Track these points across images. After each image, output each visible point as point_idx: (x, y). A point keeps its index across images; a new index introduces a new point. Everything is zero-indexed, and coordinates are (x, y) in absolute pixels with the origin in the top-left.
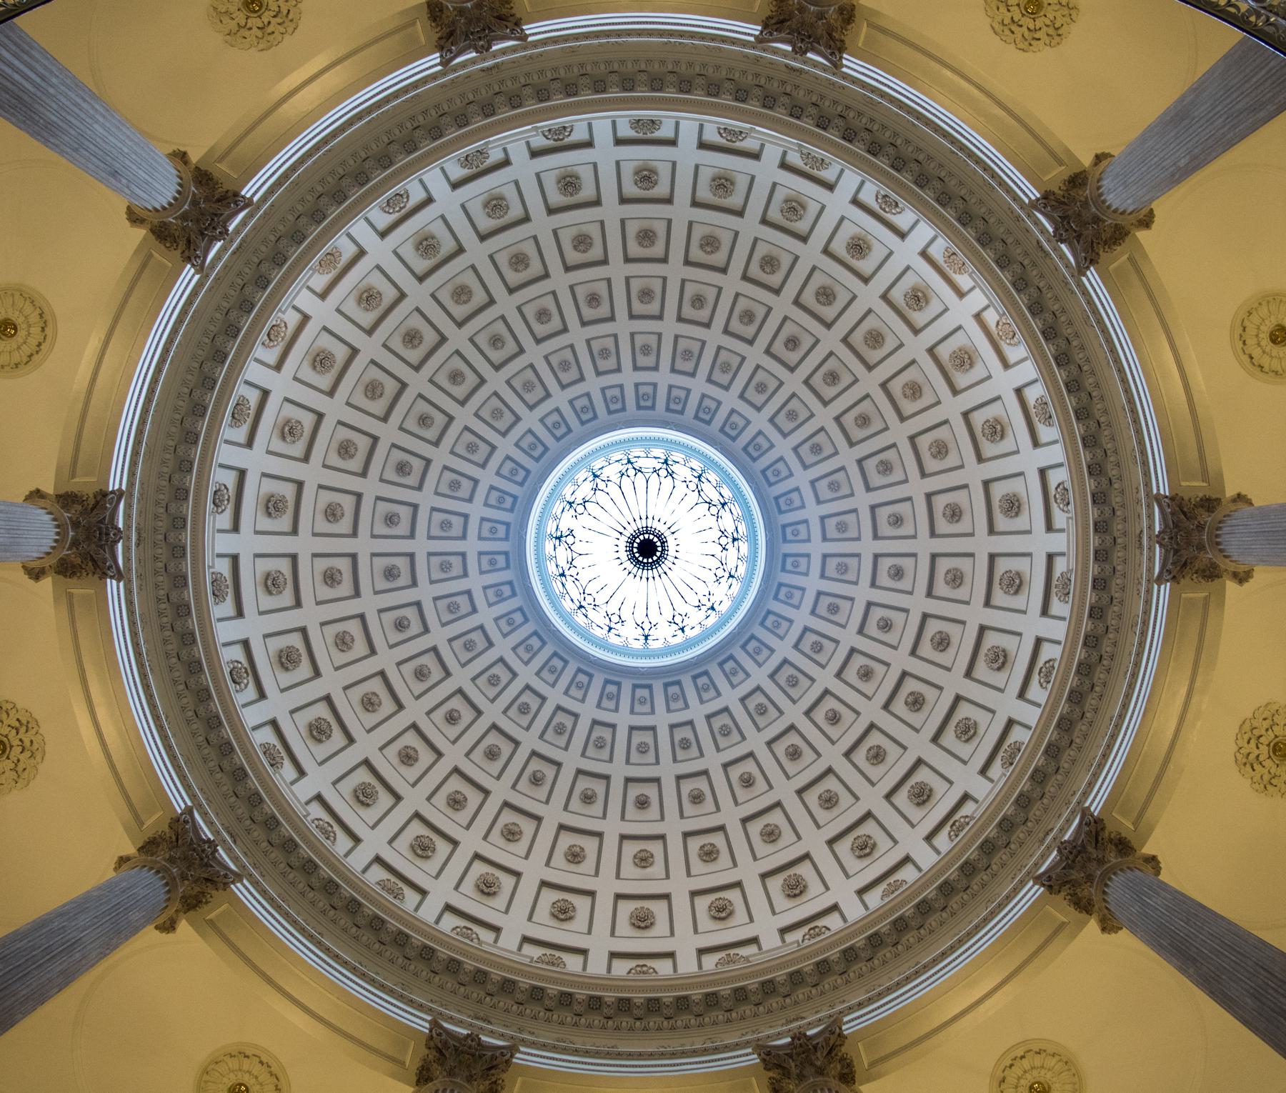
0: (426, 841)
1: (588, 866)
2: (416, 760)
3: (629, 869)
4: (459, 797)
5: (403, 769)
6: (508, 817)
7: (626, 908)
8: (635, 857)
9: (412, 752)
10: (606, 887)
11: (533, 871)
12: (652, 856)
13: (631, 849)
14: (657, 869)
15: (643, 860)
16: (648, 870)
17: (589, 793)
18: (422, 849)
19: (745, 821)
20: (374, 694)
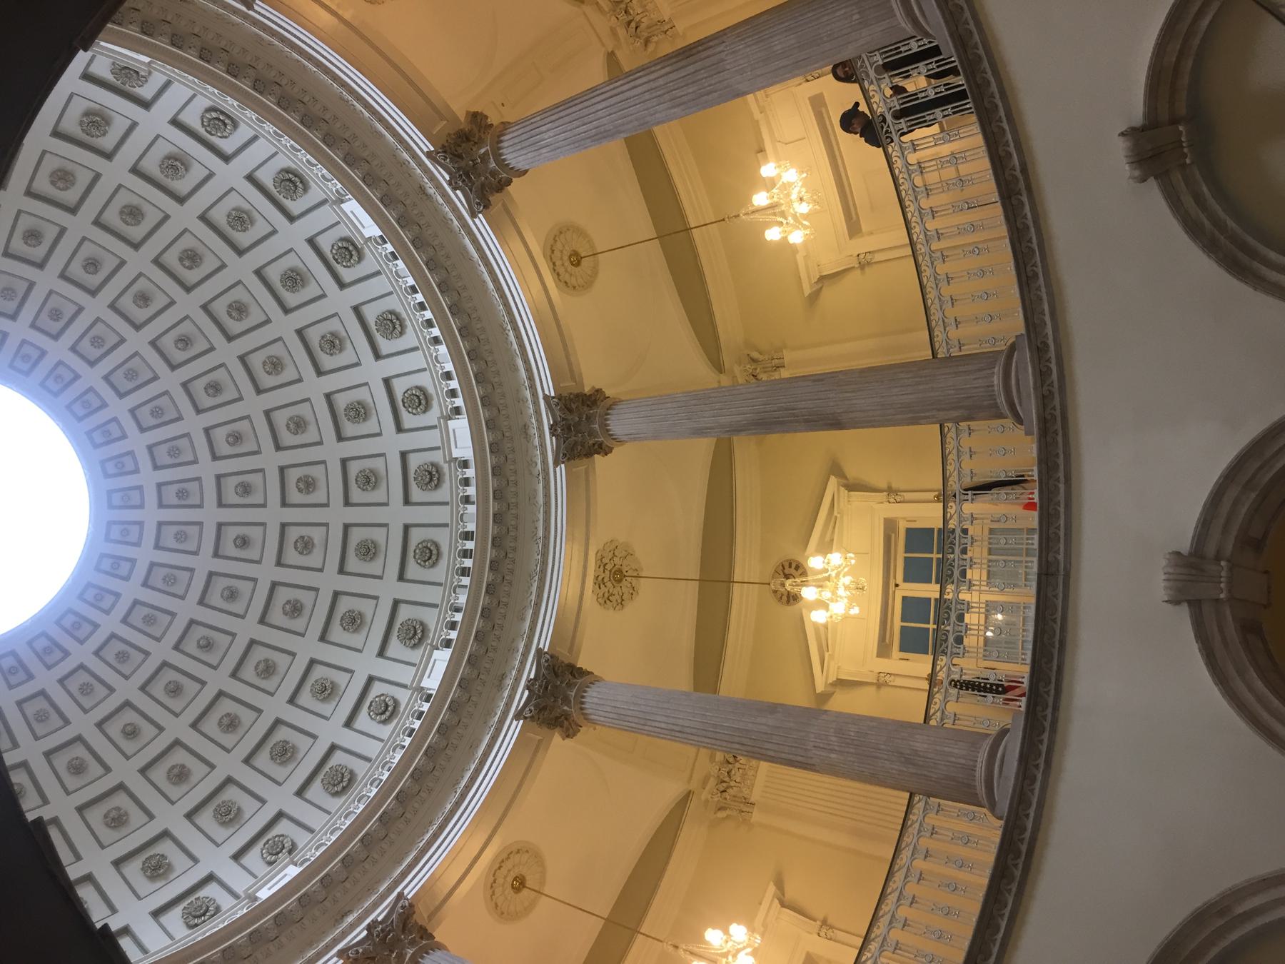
0: (279, 749)
1: (306, 598)
2: (183, 766)
3: (314, 559)
4: (226, 721)
5: (194, 779)
6: (248, 672)
7: (353, 563)
8: (301, 553)
9: (176, 771)
10: (330, 581)
11: (309, 647)
12: (302, 537)
13: (292, 556)
14: (317, 534)
15: (306, 546)
16: (316, 541)
17: (226, 593)
18: (285, 754)
19: (278, 448)
20: (106, 816)
